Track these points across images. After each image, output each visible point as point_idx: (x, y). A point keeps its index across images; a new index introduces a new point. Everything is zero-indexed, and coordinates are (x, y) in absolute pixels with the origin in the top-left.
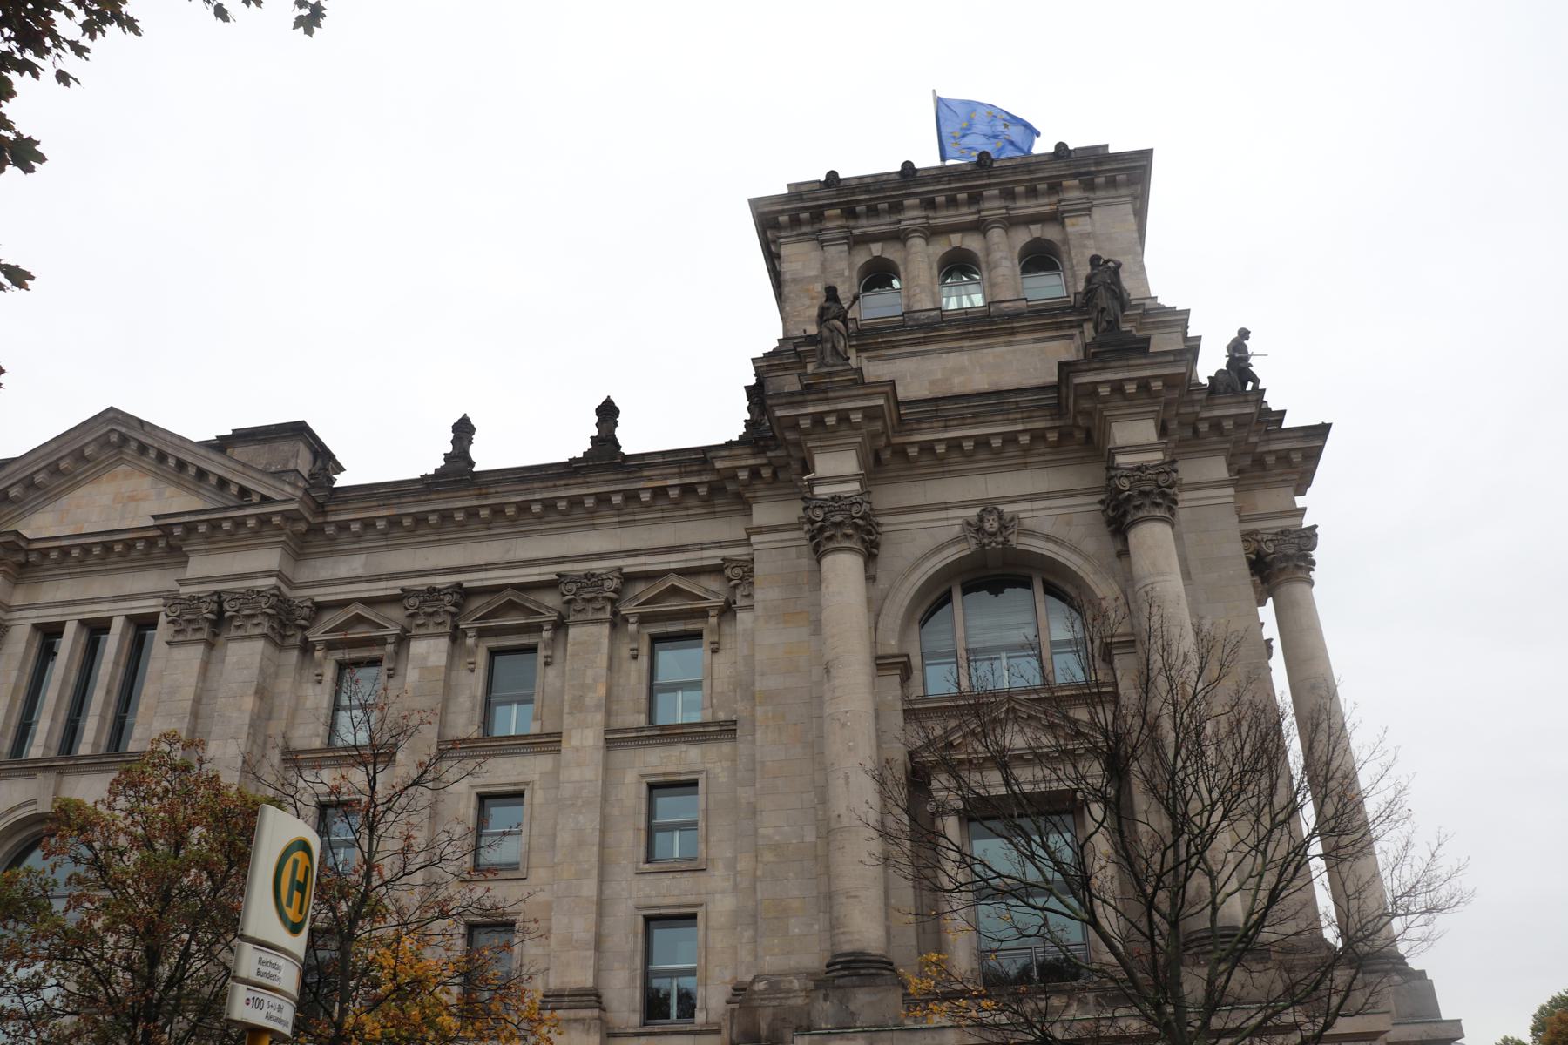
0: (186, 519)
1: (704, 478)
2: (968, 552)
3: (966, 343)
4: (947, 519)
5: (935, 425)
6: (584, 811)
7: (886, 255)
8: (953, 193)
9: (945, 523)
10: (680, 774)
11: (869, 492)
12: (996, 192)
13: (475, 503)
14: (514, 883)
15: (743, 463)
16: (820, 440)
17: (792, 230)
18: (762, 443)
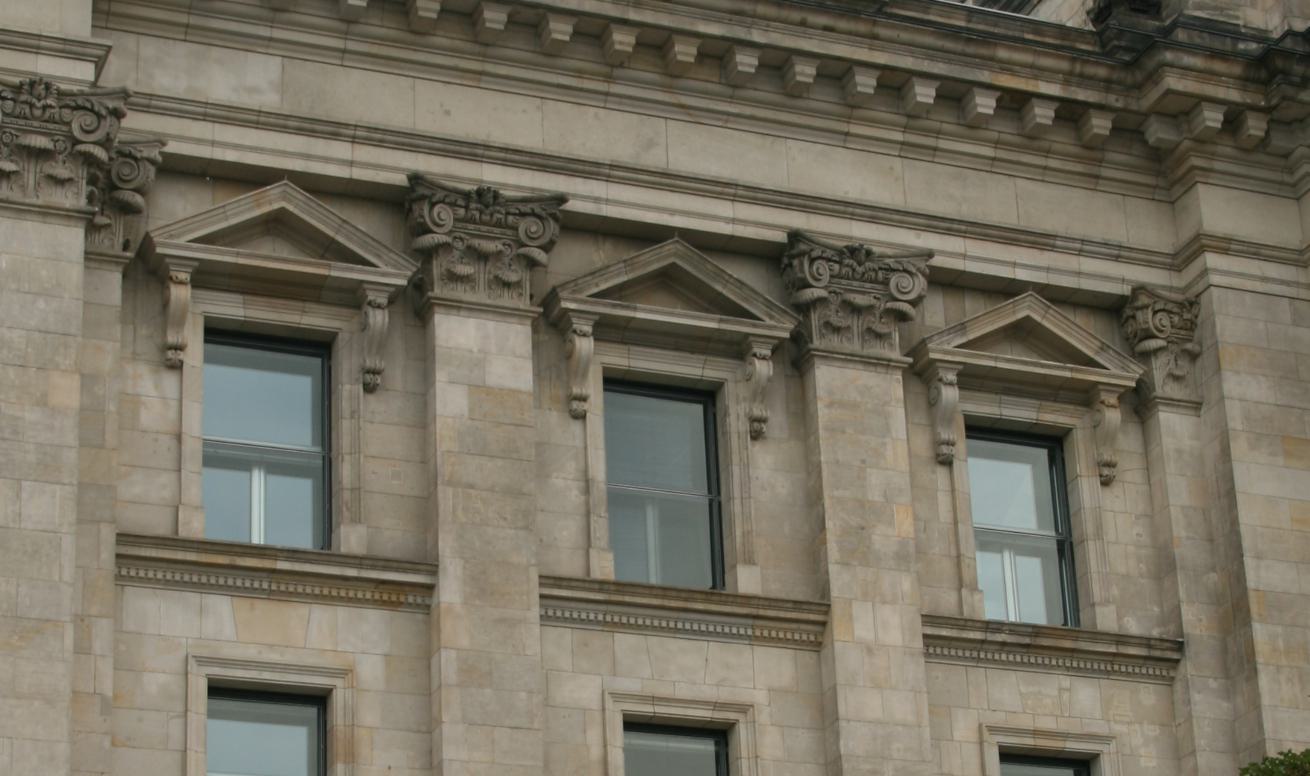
1: (1112, 100)
10: (1065, 736)
15: (1221, 93)
18: (1279, 63)
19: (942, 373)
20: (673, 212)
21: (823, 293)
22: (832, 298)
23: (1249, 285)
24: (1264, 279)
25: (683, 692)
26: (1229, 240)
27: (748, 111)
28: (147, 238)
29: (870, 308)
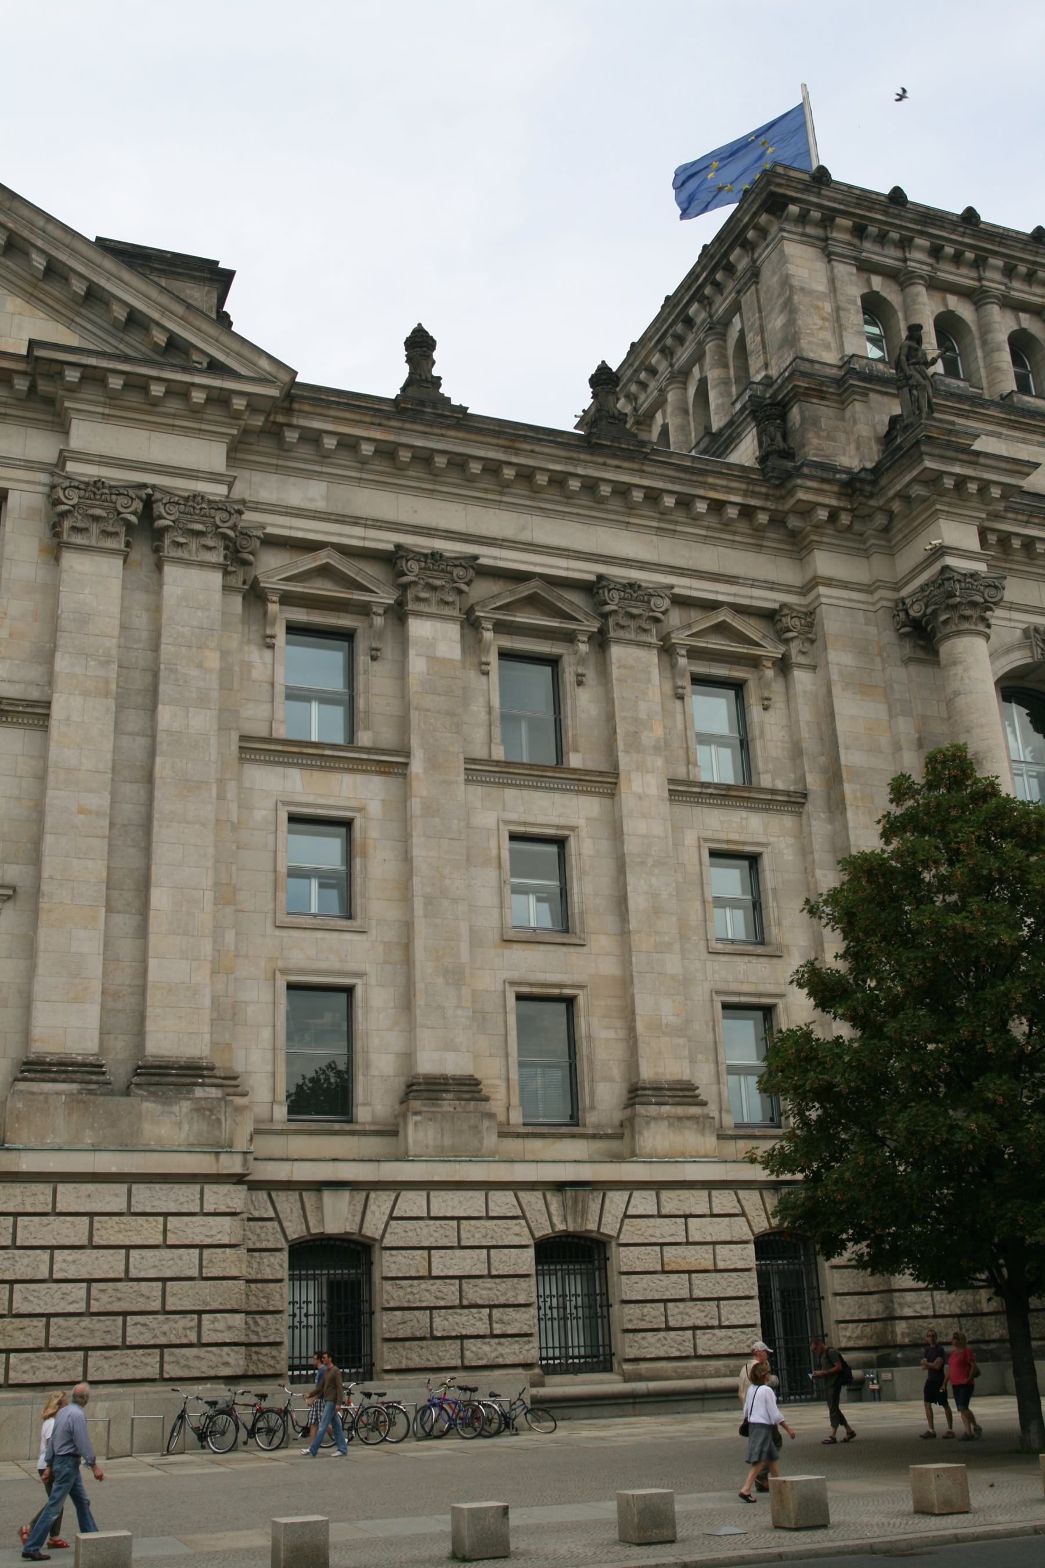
0: (92, 361)
1: (769, 505)
2: (1030, 660)
3: (1004, 431)
4: (1010, 620)
5: (1020, 517)
6: (656, 871)
7: (884, 294)
8: (963, 248)
9: (1007, 623)
10: (744, 843)
11: (1005, 578)
12: (1000, 263)
13: (501, 456)
14: (572, 949)
15: (827, 501)
16: (949, 504)
17: (795, 226)
18: (858, 485)
19: (678, 650)
20: (535, 564)
21: (615, 608)
22: (620, 610)
23: (842, 603)
24: (850, 600)
25: (541, 820)
26: (831, 579)
27: (575, 511)
28: (256, 578)
29: (640, 615)
